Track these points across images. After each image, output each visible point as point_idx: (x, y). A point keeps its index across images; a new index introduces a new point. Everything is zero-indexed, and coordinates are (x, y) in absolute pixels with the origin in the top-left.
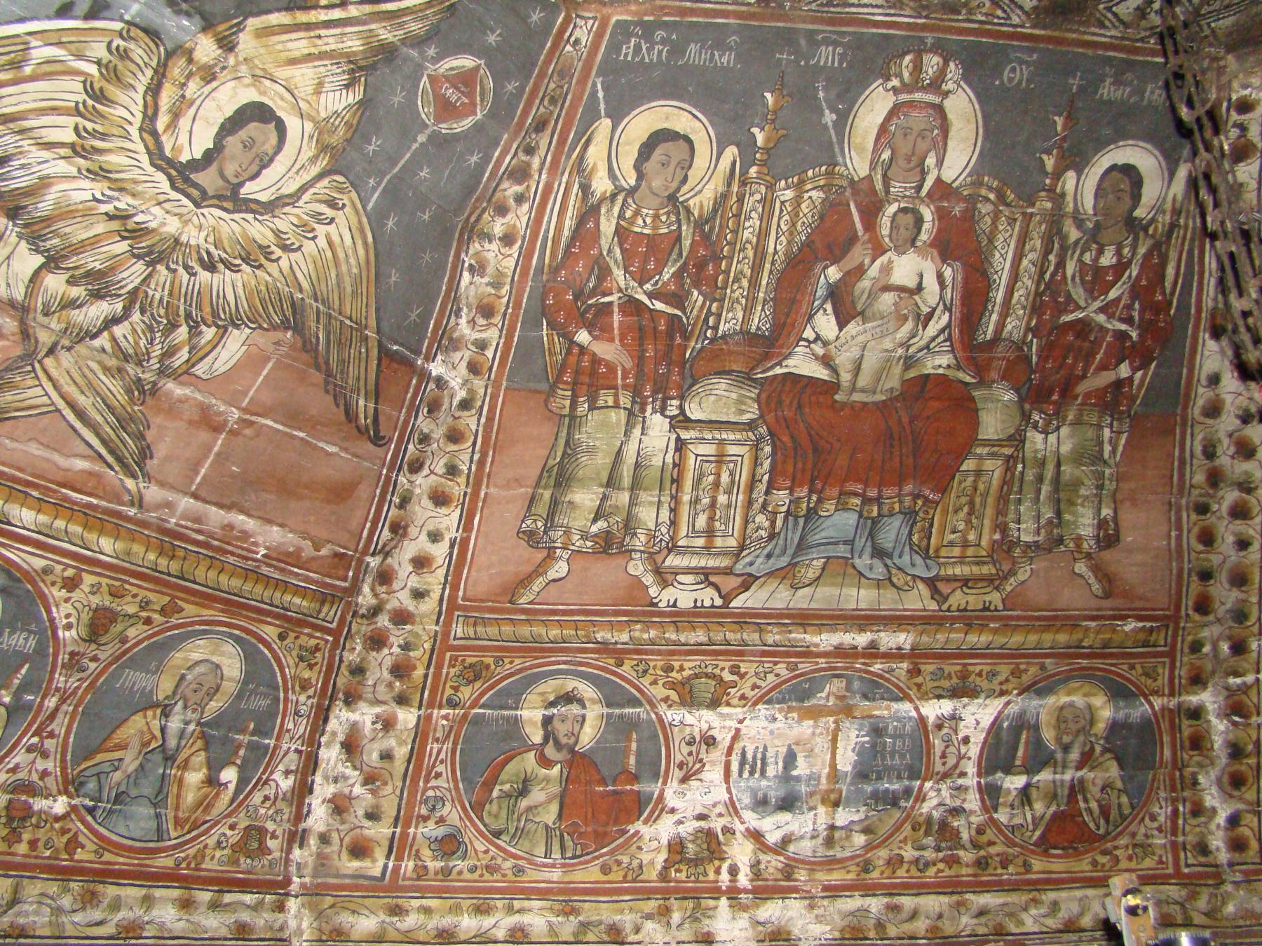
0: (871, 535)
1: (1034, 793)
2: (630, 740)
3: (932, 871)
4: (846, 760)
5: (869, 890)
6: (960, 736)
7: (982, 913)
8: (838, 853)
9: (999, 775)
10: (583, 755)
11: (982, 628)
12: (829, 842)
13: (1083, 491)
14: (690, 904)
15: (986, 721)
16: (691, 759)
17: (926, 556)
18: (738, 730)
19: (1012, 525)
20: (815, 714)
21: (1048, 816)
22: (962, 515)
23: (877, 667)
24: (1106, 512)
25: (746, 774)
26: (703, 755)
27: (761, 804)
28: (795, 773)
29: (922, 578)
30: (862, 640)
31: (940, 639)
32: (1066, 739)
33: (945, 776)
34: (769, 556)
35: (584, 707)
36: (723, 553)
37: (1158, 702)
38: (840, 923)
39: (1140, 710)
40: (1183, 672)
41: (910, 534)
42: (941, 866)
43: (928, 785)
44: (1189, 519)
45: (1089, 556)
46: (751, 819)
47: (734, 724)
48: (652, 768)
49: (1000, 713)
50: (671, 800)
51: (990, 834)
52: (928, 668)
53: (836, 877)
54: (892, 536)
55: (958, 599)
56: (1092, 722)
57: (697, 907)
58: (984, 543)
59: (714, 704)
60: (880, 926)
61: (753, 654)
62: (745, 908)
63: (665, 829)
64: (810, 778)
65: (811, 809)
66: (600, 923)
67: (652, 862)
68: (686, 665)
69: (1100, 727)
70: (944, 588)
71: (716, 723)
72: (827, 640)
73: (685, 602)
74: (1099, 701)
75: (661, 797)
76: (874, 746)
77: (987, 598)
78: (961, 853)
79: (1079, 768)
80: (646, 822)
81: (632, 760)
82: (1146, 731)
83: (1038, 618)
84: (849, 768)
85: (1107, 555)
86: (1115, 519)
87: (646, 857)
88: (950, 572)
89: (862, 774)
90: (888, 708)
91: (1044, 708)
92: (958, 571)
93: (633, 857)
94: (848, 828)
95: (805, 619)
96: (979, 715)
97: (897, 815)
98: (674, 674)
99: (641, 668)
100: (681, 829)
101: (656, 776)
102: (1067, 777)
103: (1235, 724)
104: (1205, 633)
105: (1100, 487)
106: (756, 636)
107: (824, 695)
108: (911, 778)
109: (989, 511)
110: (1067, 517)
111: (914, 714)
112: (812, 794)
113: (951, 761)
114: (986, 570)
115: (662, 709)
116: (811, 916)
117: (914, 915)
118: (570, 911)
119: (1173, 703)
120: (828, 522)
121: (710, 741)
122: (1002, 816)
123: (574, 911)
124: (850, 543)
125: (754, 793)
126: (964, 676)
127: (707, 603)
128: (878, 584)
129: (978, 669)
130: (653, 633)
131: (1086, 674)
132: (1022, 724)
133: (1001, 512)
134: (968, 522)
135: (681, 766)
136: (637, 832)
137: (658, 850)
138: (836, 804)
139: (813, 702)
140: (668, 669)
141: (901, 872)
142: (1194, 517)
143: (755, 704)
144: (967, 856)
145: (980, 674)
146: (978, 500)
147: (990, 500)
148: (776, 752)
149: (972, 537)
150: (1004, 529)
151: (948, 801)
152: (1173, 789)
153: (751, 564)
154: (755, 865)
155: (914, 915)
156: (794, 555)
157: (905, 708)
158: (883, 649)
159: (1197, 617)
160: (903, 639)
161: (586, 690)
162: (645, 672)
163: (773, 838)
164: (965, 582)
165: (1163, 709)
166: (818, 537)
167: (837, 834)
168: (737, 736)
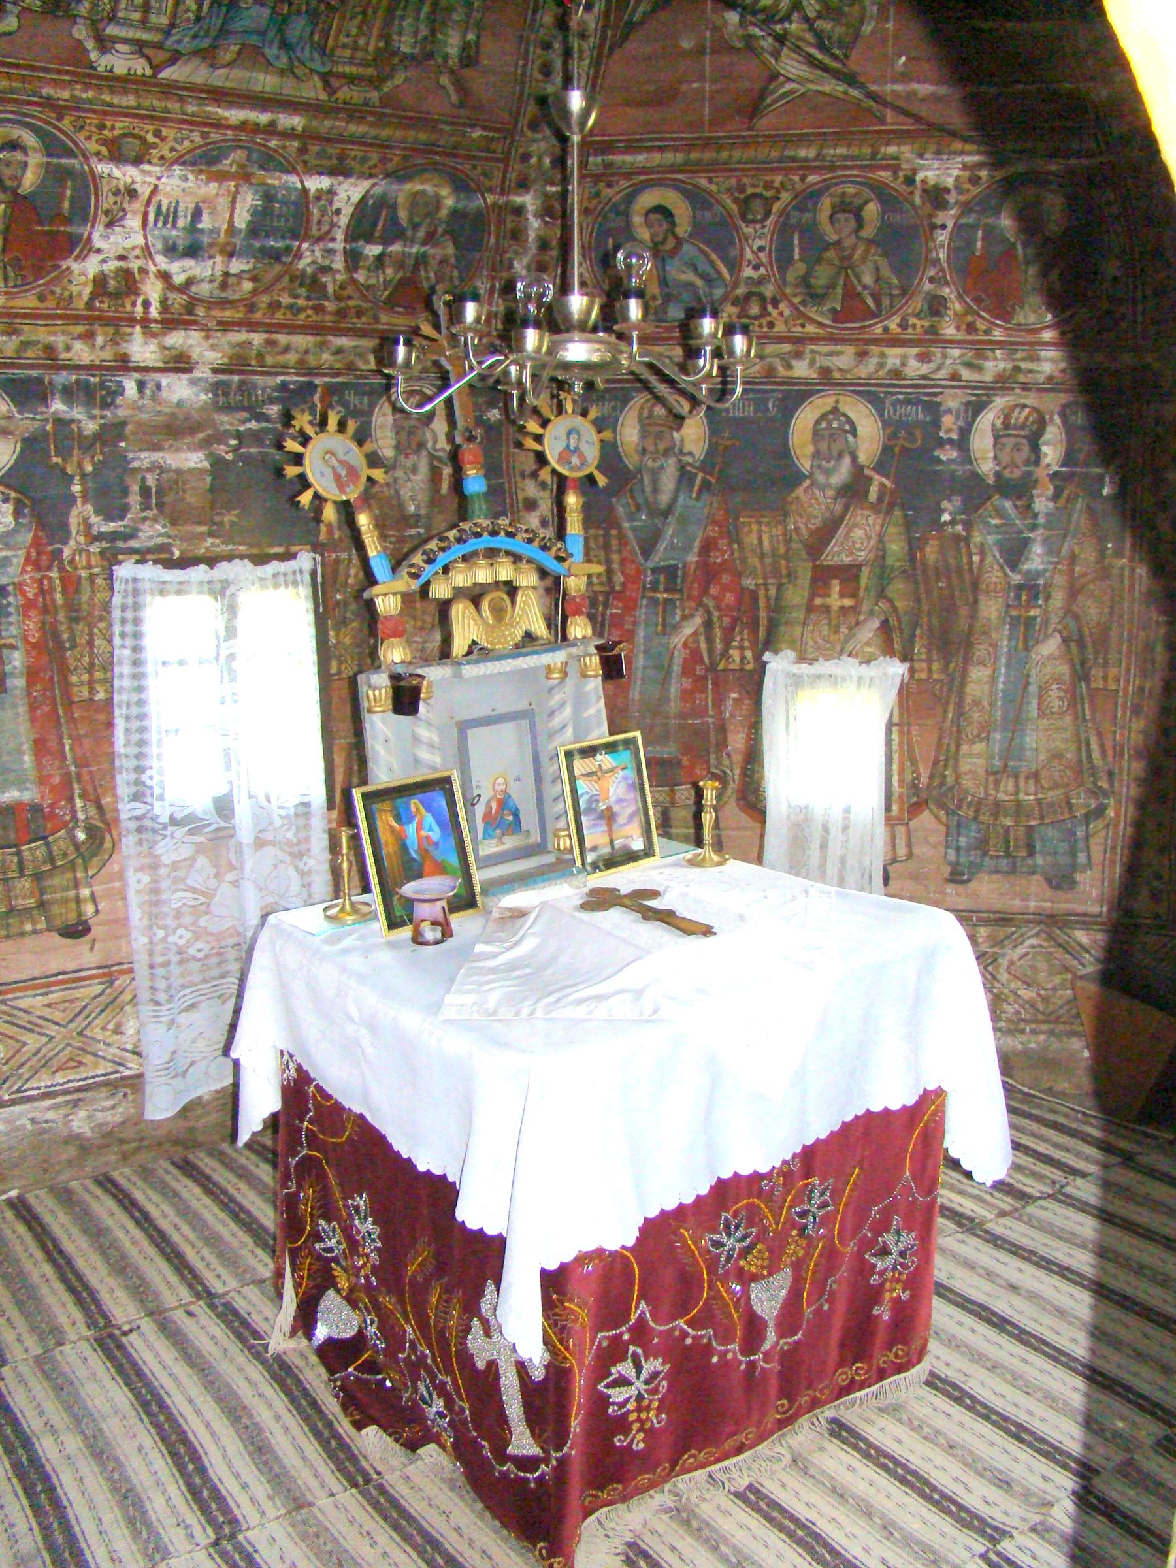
0: (280, 30)
1: (387, 261)
2: (65, 188)
3: (302, 316)
4: (242, 220)
5: (252, 326)
6: (334, 208)
7: (339, 351)
8: (229, 295)
9: (361, 243)
10: (24, 197)
11: (362, 120)
12: (224, 286)
13: (455, 17)
14: (111, 330)
15: (356, 196)
16: (116, 208)
17: (323, 53)
18: (156, 186)
19: (395, 37)
20: (220, 177)
21: (395, 282)
22: (356, 22)
23: (273, 143)
24: (471, 37)
25: (160, 224)
26: (126, 205)
27: (171, 250)
28: (200, 226)
29: (318, 73)
30: (264, 118)
31: (326, 125)
32: (417, 220)
33: (320, 239)
34: (195, 37)
35: (26, 153)
36: (158, 29)
37: (490, 199)
38: (229, 352)
39: (478, 202)
40: (513, 176)
41: (312, 34)
42: (310, 312)
43: (305, 245)
44: (535, 52)
45: (452, 72)
46: (162, 261)
47: (153, 180)
48: (82, 213)
49: (367, 192)
50: (98, 243)
51: (350, 290)
52: (314, 149)
53: (228, 314)
54: (297, 33)
55: (344, 93)
56: (438, 206)
57: (117, 332)
58: (371, 49)
59: (137, 161)
60: (260, 357)
61: (173, 120)
62: (154, 335)
63: (92, 266)
64: (212, 231)
65: (211, 257)
66: (38, 342)
67: (80, 295)
68: (118, 125)
69: (444, 213)
70: (335, 82)
71: (139, 178)
72: (235, 115)
73: (120, 69)
74: (444, 192)
75: (89, 239)
76: (265, 208)
77: (368, 95)
78: (326, 303)
79: (424, 244)
80: (76, 260)
81: (66, 205)
82: (479, 221)
83: (406, 118)
84: (243, 226)
85: (467, 72)
86: (477, 44)
87: (75, 289)
88: (341, 69)
89: (254, 231)
90: (279, 179)
91: (403, 192)
92: (347, 69)
93: (64, 289)
94: (239, 276)
95: (218, 95)
96: (350, 192)
97: (278, 268)
98: (106, 132)
99: (80, 123)
100: (105, 267)
101: (85, 221)
102: (414, 250)
103: (546, 223)
104: (534, 148)
105: (469, 16)
106: (177, 106)
107: (228, 162)
108: (294, 237)
109: (378, 23)
110: (439, 36)
111: (299, 185)
112: (211, 245)
113: (325, 228)
114: (370, 71)
115: (94, 161)
116: (206, 345)
117: (287, 349)
118: (12, 332)
119: (502, 200)
120: (246, 14)
121: (132, 193)
122: (360, 276)
123: (15, 332)
124: (262, 33)
125: (165, 240)
126: (341, 158)
127: (139, 72)
128: (282, 73)
129: (353, 153)
130: (90, 94)
131: (436, 168)
132: (384, 204)
133: (388, 23)
134: (360, 27)
135: (107, 213)
136: (68, 268)
137: (84, 284)
138: (231, 255)
139: (219, 167)
140: (102, 127)
141: (279, 315)
142: (539, 51)
143: (172, 164)
144: (330, 306)
145: (355, 158)
146: (370, 11)
147: (381, 12)
148: (186, 206)
149: (361, 42)
150: (386, 37)
151: (320, 260)
152: (494, 270)
153: (179, 42)
154: (163, 301)
155: (287, 349)
156: (215, 38)
157: (293, 180)
158: (280, 128)
159: (529, 134)
160: (296, 121)
161: (29, 139)
162: (82, 128)
163: (179, 279)
164: (352, 80)
165: (494, 204)
166: (238, 25)
167: (231, 280)
168: (155, 190)
